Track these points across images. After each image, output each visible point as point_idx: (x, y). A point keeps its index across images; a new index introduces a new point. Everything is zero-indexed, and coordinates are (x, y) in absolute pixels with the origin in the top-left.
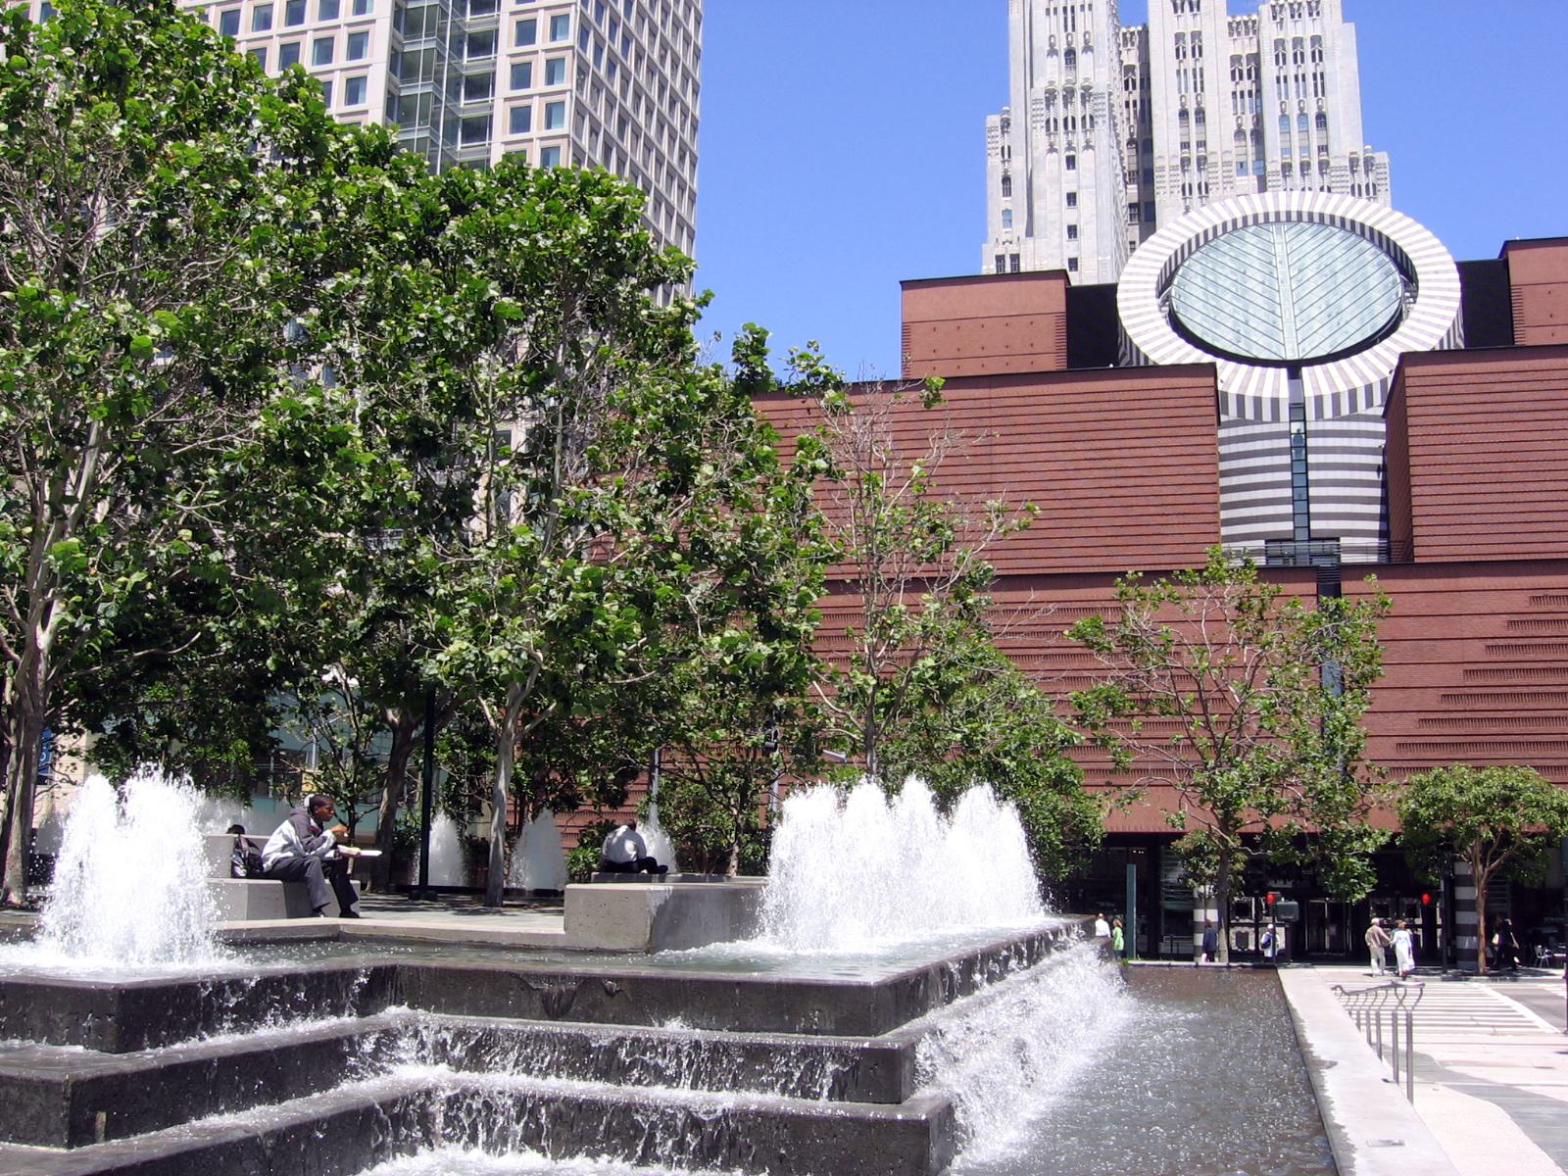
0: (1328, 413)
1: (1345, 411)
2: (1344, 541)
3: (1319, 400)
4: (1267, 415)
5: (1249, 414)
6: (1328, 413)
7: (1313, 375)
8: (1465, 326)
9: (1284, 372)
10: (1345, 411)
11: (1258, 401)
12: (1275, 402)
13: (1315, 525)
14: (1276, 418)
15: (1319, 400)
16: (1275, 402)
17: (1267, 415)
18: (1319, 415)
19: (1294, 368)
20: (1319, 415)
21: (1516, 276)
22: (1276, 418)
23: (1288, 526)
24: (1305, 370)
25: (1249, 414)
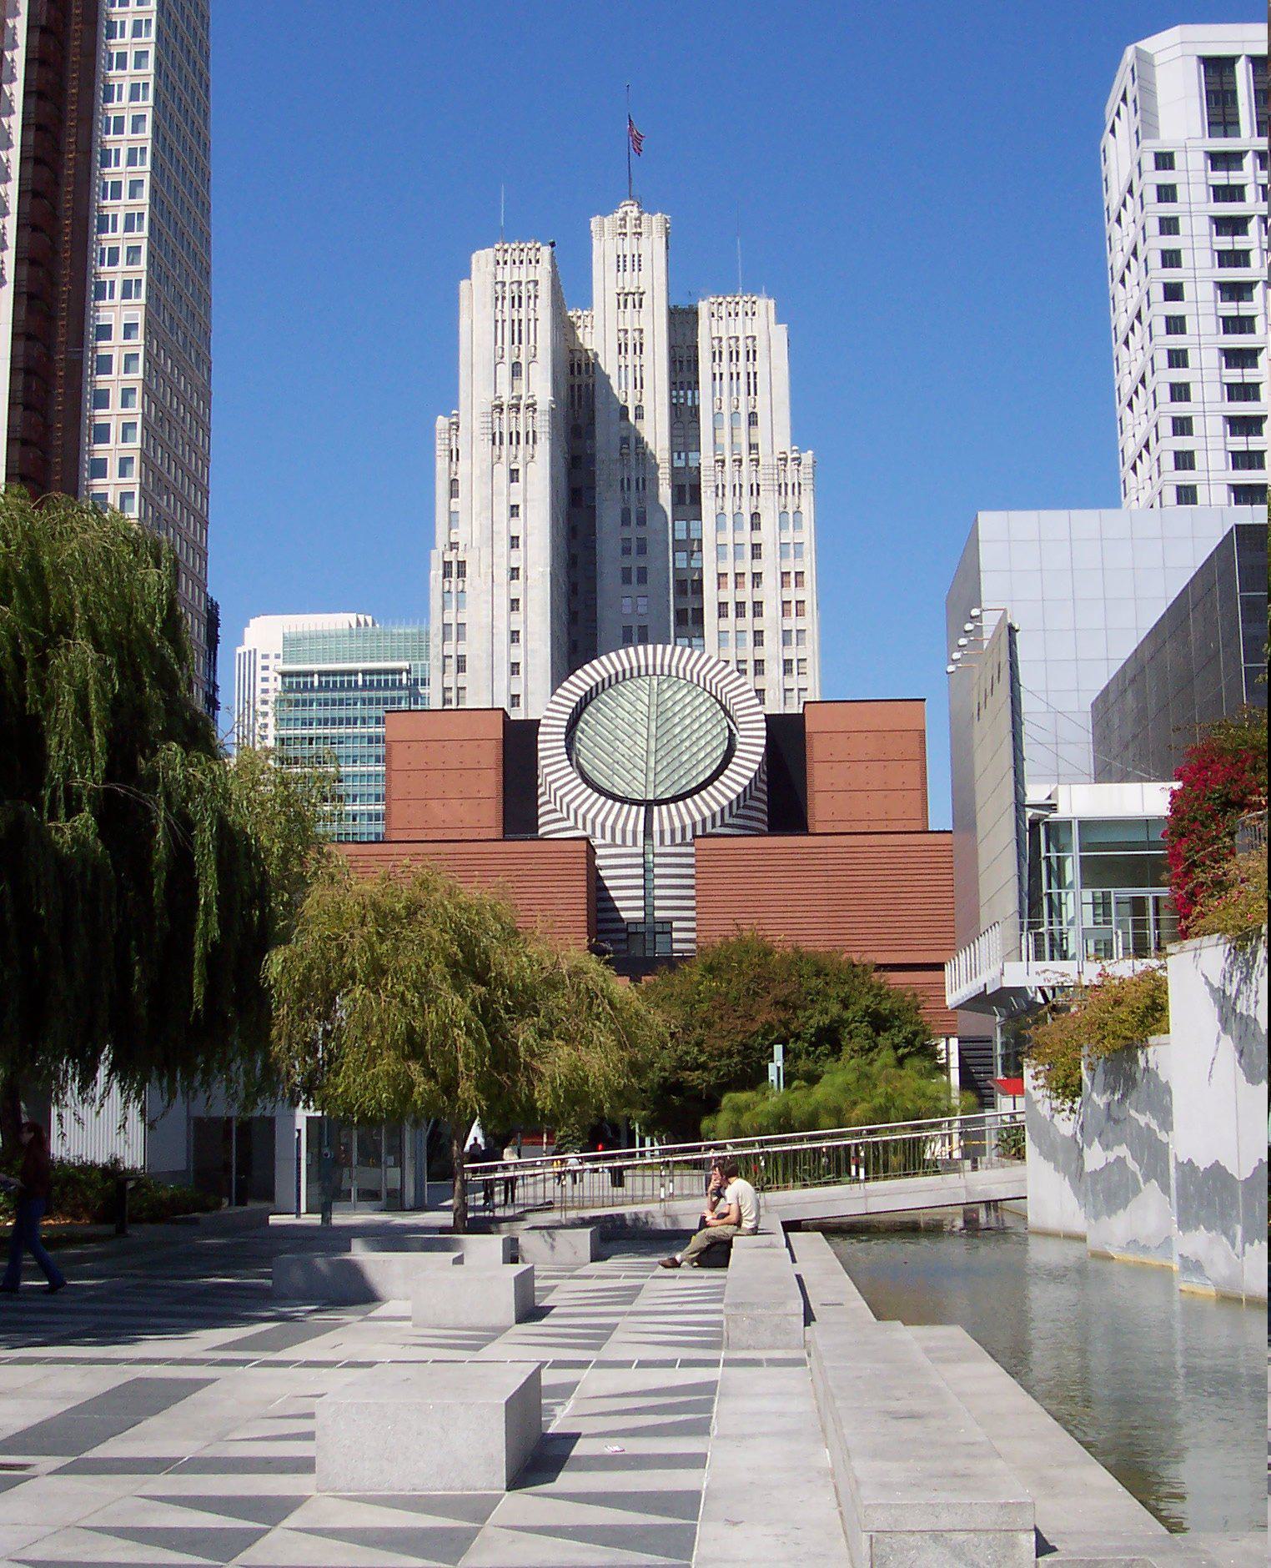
0: (668, 841)
1: (678, 840)
2: (675, 924)
3: (662, 832)
4: (629, 842)
5: (619, 841)
6: (668, 841)
7: (660, 813)
8: (768, 774)
9: (643, 809)
10: (678, 840)
11: (624, 831)
12: (635, 833)
13: (658, 914)
14: (635, 844)
15: (662, 832)
16: (635, 833)
17: (629, 842)
18: (662, 843)
19: (649, 805)
20: (662, 843)
21: (809, 727)
22: (635, 844)
23: (641, 914)
24: (656, 809)
25: (619, 841)
